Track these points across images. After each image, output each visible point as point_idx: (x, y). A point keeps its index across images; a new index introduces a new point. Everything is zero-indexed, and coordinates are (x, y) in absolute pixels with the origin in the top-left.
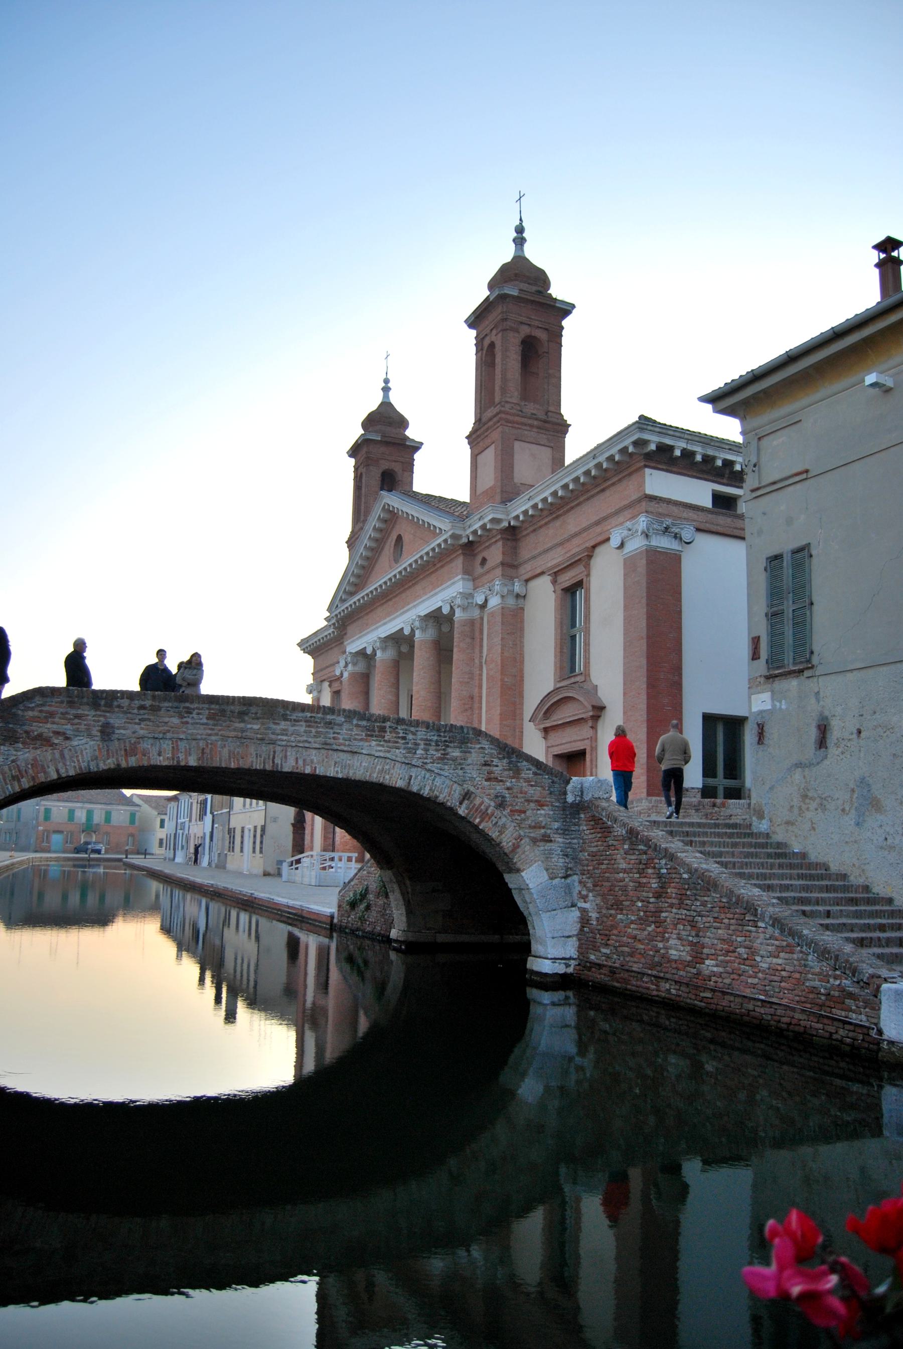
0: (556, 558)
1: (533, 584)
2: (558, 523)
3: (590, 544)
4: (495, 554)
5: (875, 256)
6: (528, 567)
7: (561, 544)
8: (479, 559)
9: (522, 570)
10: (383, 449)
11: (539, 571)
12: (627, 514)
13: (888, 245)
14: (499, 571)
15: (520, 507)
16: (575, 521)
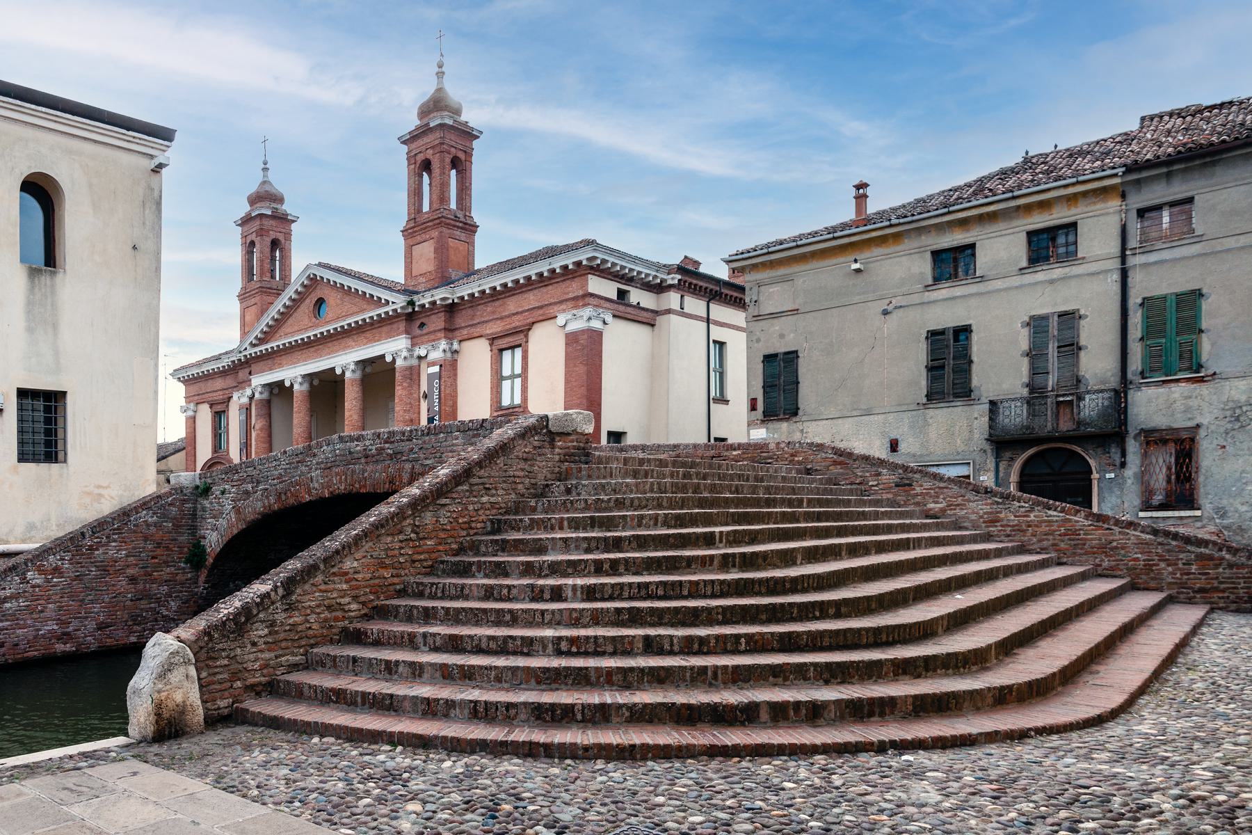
0: (495, 328)
1: (465, 344)
2: (497, 303)
3: (531, 320)
4: (437, 322)
5: (853, 192)
6: (465, 332)
7: (502, 318)
8: (418, 323)
9: (457, 333)
10: (272, 222)
11: (476, 334)
12: (570, 304)
13: (861, 186)
14: (442, 334)
15: (465, 290)
16: (512, 305)
